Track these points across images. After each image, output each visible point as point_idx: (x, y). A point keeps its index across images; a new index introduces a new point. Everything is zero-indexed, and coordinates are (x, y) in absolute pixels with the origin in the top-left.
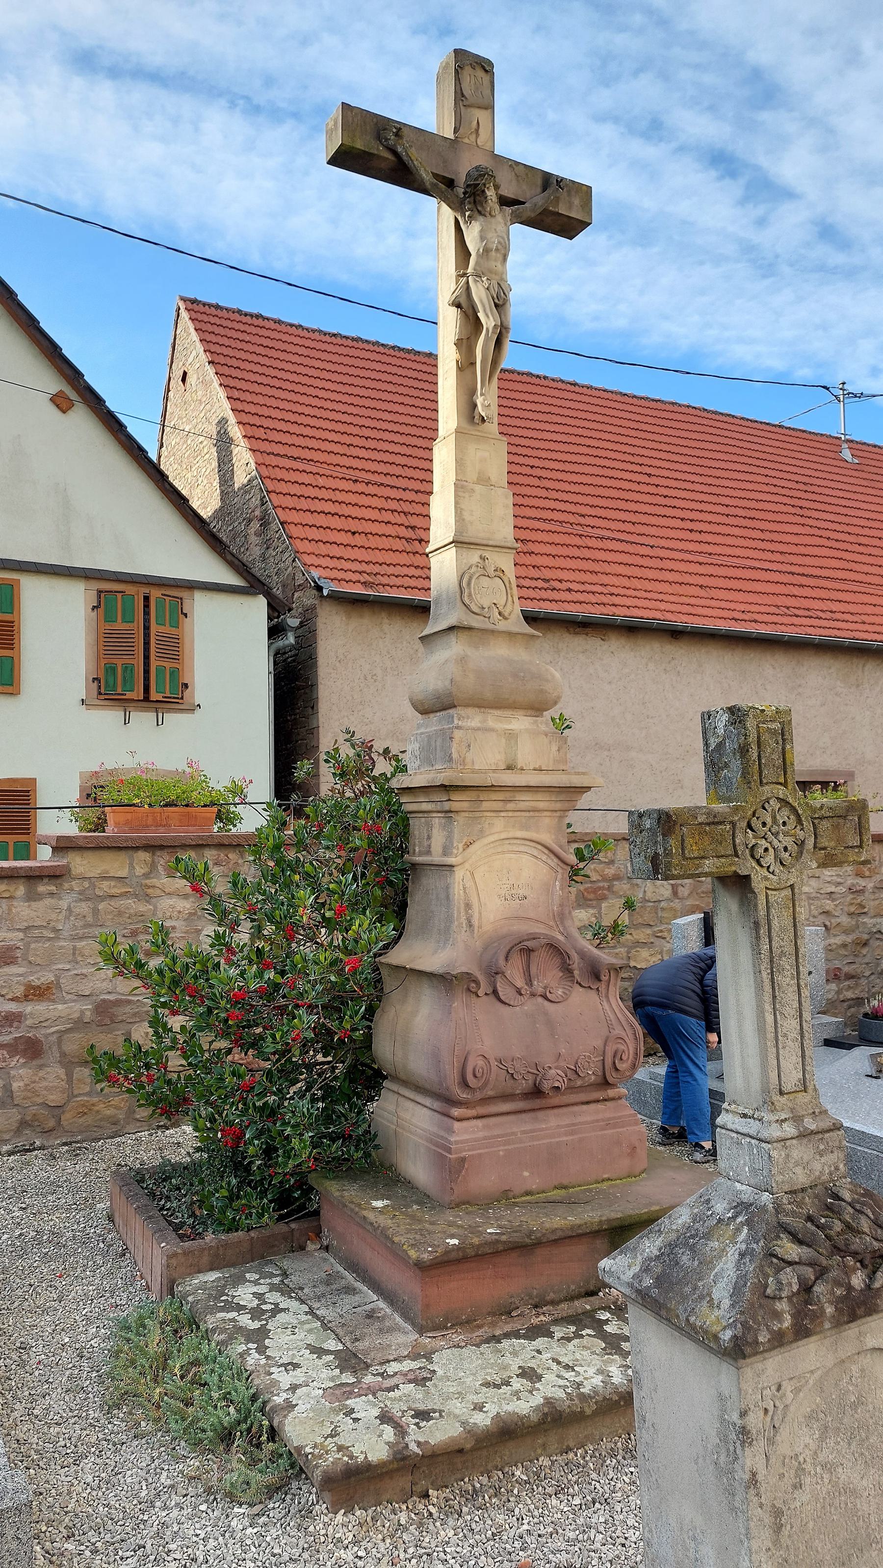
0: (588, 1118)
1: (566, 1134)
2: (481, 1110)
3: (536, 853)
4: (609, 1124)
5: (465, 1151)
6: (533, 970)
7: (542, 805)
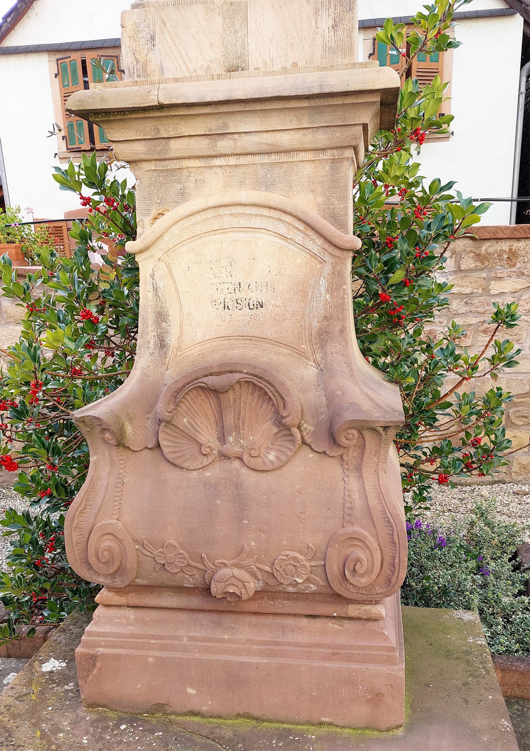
0: (304, 639)
1: (260, 654)
2: (134, 599)
3: (283, 230)
4: (336, 653)
5: (101, 646)
6: (229, 420)
7: (286, 140)
